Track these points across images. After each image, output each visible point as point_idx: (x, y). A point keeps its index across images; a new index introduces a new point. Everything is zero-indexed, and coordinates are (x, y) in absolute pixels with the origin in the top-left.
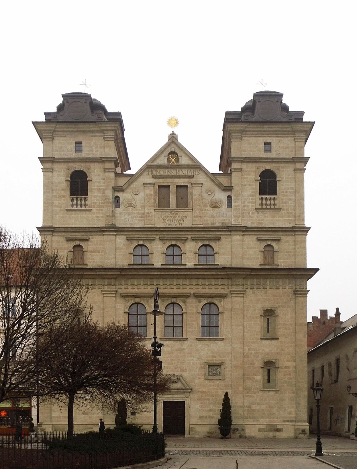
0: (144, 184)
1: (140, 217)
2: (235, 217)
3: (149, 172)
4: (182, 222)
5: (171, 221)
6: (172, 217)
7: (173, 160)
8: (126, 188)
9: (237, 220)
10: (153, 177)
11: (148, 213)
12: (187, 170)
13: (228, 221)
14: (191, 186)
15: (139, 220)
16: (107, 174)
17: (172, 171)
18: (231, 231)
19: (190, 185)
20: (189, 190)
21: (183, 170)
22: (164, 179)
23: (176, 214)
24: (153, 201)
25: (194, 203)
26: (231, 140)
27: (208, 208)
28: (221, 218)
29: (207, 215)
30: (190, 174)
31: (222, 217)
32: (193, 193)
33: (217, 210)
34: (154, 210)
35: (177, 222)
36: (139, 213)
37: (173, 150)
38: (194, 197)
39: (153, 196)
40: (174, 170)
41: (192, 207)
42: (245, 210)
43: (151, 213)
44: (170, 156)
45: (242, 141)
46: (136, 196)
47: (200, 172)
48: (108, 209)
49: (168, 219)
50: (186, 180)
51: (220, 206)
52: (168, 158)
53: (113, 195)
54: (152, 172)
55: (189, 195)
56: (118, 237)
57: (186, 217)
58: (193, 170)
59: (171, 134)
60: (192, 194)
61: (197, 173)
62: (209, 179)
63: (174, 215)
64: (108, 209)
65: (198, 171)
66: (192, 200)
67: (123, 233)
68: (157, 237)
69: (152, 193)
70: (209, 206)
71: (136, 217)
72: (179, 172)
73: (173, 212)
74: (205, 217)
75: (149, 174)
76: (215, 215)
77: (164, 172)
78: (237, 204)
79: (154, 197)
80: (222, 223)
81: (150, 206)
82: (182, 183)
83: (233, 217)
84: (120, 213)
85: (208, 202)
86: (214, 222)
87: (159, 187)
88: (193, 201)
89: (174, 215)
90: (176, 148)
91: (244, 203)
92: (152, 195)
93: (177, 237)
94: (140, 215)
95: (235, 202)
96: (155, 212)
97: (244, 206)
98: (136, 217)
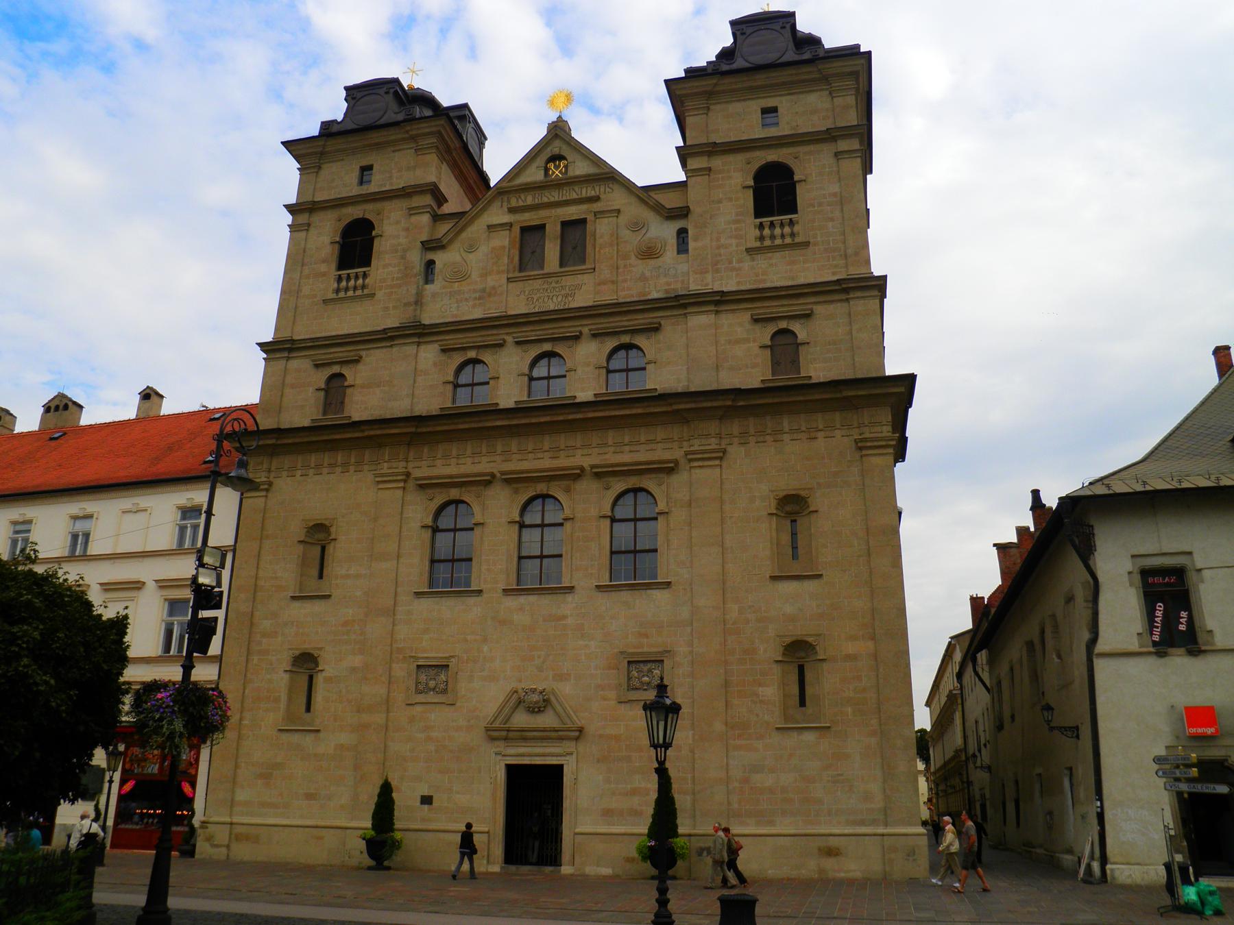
0: (489, 227)
1: (475, 299)
2: (696, 273)
3: (502, 202)
4: (570, 299)
5: (546, 300)
6: (547, 290)
7: (557, 172)
8: (451, 241)
9: (702, 281)
10: (512, 210)
11: (494, 288)
12: (587, 187)
13: (679, 286)
14: (593, 218)
15: (474, 306)
16: (414, 218)
17: (553, 193)
18: (685, 306)
19: (590, 217)
20: (589, 227)
21: (576, 188)
22: (533, 213)
23: (557, 282)
24: (506, 260)
25: (599, 251)
26: (684, 113)
27: (633, 260)
28: (663, 280)
29: (629, 277)
30: (593, 193)
31: (665, 276)
32: (598, 231)
33: (652, 262)
34: (508, 279)
35: (559, 299)
36: (475, 291)
37: (556, 151)
38: (599, 241)
39: (507, 250)
40: (557, 190)
41: (595, 264)
42: (720, 255)
43: (500, 286)
44: (551, 166)
45: (710, 114)
46: (471, 256)
47: (616, 187)
48: (408, 289)
49: (538, 295)
50: (584, 207)
51: (662, 251)
52: (546, 170)
53: (421, 259)
54: (509, 201)
55: (588, 238)
56: (423, 347)
57: (579, 287)
58: (600, 185)
59: (553, 122)
60: (594, 235)
61: (608, 189)
62: (633, 200)
63: (554, 285)
64: (408, 289)
65: (611, 185)
66: (595, 249)
67: (435, 338)
68: (509, 339)
69: (506, 243)
70: (633, 257)
71: (466, 300)
72: (567, 194)
73: (550, 280)
74: (625, 281)
75: (502, 206)
76: (648, 274)
77: (534, 198)
78: (699, 244)
79: (509, 251)
80: (667, 291)
81: (499, 272)
82: (573, 214)
83: (691, 273)
84: (434, 295)
85: (631, 249)
86: (647, 290)
87: (525, 230)
88: (597, 249)
89: (554, 285)
90: (564, 147)
91: (718, 239)
92: (504, 247)
93: (553, 334)
94: (477, 295)
95: (696, 240)
96: (511, 285)
97: (718, 247)
98: (466, 300)
